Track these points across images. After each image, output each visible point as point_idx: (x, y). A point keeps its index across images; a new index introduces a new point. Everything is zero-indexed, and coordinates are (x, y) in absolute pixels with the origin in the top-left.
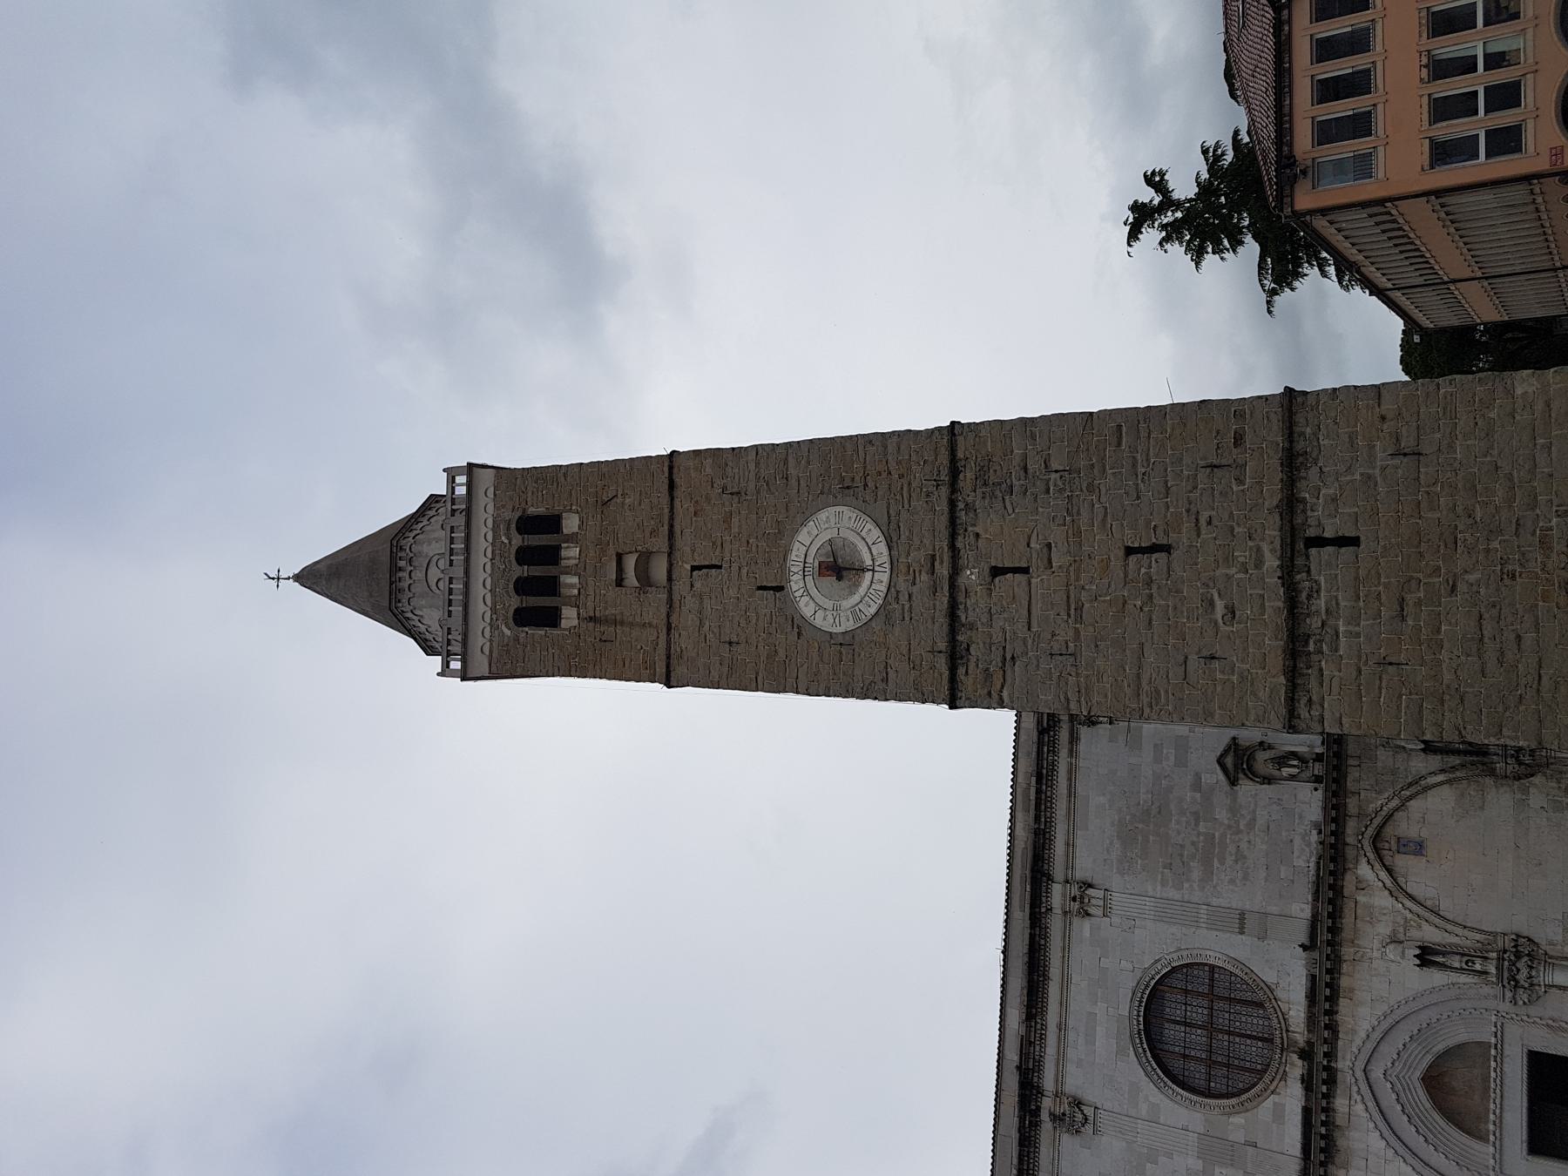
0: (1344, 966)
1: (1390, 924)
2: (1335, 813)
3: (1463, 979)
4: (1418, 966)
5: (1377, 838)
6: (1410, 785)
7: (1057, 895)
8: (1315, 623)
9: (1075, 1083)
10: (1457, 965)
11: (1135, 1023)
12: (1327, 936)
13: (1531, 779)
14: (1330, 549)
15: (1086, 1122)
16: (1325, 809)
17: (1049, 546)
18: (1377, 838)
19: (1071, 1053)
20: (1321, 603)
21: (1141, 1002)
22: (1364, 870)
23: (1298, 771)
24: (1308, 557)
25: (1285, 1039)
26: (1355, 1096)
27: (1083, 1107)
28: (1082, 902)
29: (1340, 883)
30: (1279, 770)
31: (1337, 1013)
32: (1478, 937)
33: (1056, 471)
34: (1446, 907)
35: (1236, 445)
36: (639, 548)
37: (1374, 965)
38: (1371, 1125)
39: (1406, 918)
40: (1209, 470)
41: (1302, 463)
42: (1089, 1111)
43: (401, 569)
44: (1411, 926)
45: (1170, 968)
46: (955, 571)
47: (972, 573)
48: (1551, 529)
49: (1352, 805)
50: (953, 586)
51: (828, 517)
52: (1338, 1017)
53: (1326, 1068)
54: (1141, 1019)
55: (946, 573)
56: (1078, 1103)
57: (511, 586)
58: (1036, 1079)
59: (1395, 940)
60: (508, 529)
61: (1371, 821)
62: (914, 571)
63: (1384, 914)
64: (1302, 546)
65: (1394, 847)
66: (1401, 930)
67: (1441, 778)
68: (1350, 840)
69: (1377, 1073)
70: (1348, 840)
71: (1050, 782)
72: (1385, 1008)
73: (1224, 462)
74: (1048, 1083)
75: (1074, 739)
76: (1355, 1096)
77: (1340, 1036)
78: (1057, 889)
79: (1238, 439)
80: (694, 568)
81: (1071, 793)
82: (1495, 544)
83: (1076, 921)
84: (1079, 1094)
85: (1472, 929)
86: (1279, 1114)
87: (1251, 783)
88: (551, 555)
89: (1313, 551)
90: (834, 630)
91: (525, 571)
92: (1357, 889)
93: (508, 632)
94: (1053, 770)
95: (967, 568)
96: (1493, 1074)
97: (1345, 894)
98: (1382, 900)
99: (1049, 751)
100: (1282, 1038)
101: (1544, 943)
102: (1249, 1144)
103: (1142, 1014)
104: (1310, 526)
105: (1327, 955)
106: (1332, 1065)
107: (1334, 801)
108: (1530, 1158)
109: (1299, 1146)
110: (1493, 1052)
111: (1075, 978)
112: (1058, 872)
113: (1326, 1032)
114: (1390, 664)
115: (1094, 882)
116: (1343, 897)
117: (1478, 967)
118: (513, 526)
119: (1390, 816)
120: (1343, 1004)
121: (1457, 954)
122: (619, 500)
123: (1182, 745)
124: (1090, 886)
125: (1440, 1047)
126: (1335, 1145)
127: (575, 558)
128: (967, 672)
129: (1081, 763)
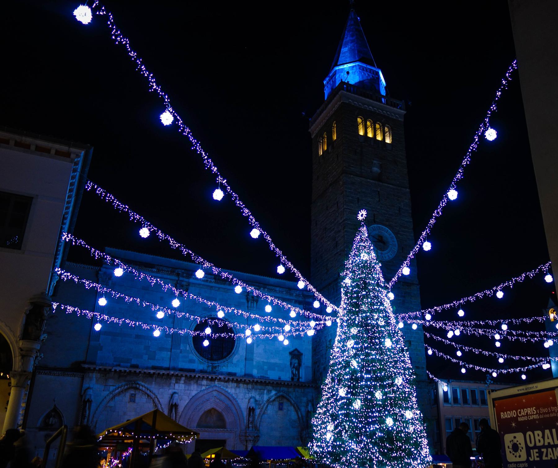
0: (246, 385)
1: (259, 400)
4: (250, 407)
5: (283, 397)
6: (298, 407)
10: (251, 419)
16: (273, 380)
18: (283, 397)
22: (274, 392)
23: (294, 373)
25: (215, 365)
30: (294, 367)
31: (232, 382)
39: (261, 404)
49: (291, 390)
52: (231, 383)
61: (288, 395)
65: (281, 402)
66: (258, 403)
67: (300, 416)
77: (225, 383)
97: (267, 387)
98: (266, 397)
100: (215, 364)
106: (216, 380)
110: (225, 430)
117: (250, 425)
120: (235, 384)
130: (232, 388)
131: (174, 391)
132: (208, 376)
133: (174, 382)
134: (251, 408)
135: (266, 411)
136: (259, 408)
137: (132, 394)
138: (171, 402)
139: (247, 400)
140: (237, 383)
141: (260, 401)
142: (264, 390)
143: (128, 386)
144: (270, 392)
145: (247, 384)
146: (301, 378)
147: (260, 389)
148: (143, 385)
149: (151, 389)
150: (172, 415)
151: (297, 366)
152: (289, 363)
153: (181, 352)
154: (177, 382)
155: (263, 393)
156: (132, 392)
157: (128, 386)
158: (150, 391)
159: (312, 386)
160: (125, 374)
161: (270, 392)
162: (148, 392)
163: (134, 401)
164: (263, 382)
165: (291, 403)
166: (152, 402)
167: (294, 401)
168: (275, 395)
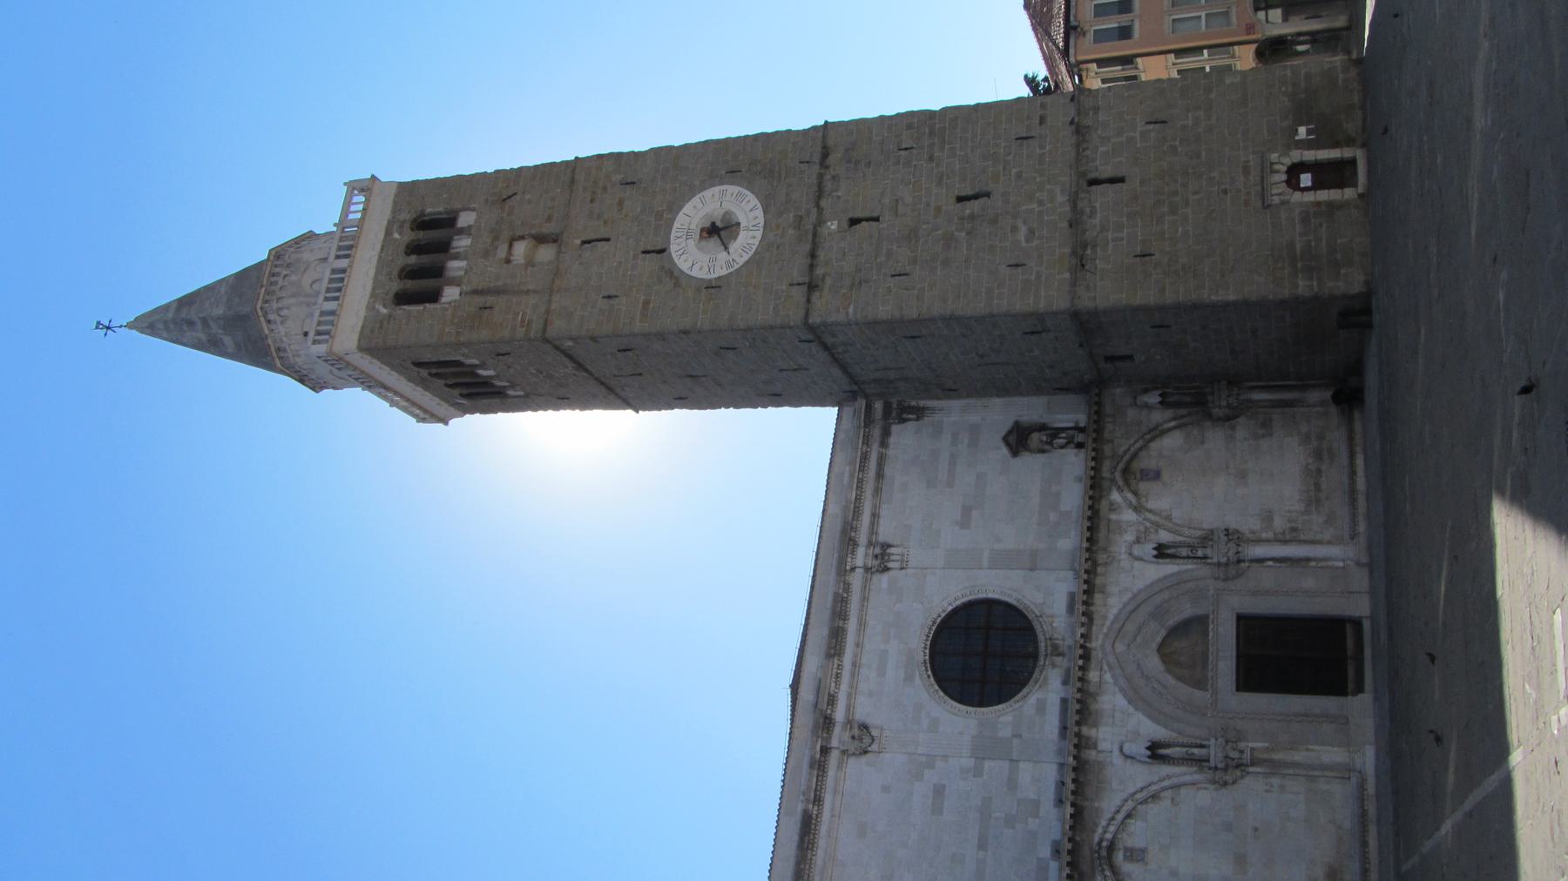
0: (1099, 570)
2: (1097, 459)
3: (1188, 566)
4: (1156, 557)
6: (1150, 431)
7: (861, 557)
8: (1090, 235)
9: (865, 710)
10: (1184, 552)
11: (922, 654)
12: (1085, 545)
13: (1237, 420)
14: (1104, 185)
15: (872, 743)
17: (897, 200)
19: (862, 686)
20: (1097, 221)
21: (928, 636)
22: (1115, 496)
23: (1064, 441)
24: (1089, 192)
26: (1105, 667)
27: (872, 730)
28: (882, 559)
29: (1097, 507)
30: (1050, 443)
31: (1092, 604)
32: (1199, 533)
33: (906, 149)
34: (1176, 514)
35: (1041, 123)
36: (533, 232)
37: (1123, 564)
38: (1117, 689)
39: (1146, 528)
40: (1020, 141)
41: (1086, 132)
42: (875, 733)
43: (273, 275)
44: (1150, 532)
45: (954, 606)
46: (820, 222)
47: (832, 224)
48: (1248, 161)
49: (1107, 449)
50: (815, 235)
51: (713, 195)
53: (1082, 647)
54: (927, 651)
55: (811, 227)
56: (864, 727)
57: (395, 273)
58: (829, 711)
59: (1138, 541)
60: (401, 227)
62: (784, 228)
63: (1130, 526)
64: (1085, 184)
65: (1138, 476)
66: (1143, 536)
67: (1173, 424)
68: (1106, 474)
69: (1120, 647)
70: (1104, 475)
71: (862, 468)
72: (1129, 595)
73: (1030, 135)
74: (839, 715)
75: (886, 433)
76: (1105, 667)
77: (1095, 622)
78: (861, 551)
79: (1042, 120)
80: (584, 242)
81: (880, 475)
82: (1215, 174)
83: (876, 577)
84: (869, 721)
85: (1195, 529)
86: (1041, 708)
87: (1027, 453)
88: (443, 247)
89: (1094, 188)
90: (709, 277)
91: (413, 259)
92: (1110, 509)
93: (384, 311)
94: (865, 458)
95: (830, 221)
96: (1211, 634)
97: (1102, 514)
98: (1129, 516)
99: (863, 443)
101: (1248, 532)
102: (1015, 736)
103: (928, 647)
104: (1091, 172)
105: (1087, 560)
106: (1088, 645)
107: (1094, 445)
108: (1238, 693)
109: (1056, 731)
110: (1211, 617)
111: (871, 622)
112: (862, 538)
113: (1084, 618)
114: (1144, 256)
115: (895, 543)
116: (1099, 517)
117: (1200, 553)
118: (407, 225)
119: (1135, 455)
120: (1098, 597)
121: (1184, 547)
122: (518, 197)
123: (974, 431)
124: (890, 546)
125: (1171, 622)
126: (1088, 708)
127: (467, 246)
128: (821, 296)
129: (890, 452)
130: (1105, 605)
131: (1116, 753)
132: (1077, 668)
133: (1093, 753)
134: (1155, 552)
135: (1164, 514)
136: (1157, 531)
137: (1125, 856)
138: (1143, 759)
139: (1137, 564)
140: (1093, 592)
141: (1138, 531)
142: (1109, 520)
143: (1105, 867)
144: (1115, 506)
145: (1095, 564)
146: (1077, 422)
147: (1109, 531)
148: (1102, 831)
149: (1113, 810)
150: (1177, 756)
151: (1046, 435)
152: (1041, 458)
153: (1019, 736)
154: (1095, 746)
155: (1118, 522)
156: (1119, 857)
157: (1105, 867)
158: (1118, 812)
159: (1098, 395)
160: (1076, 876)
161: (1115, 506)
162: (1120, 817)
163: (1143, 851)
164: (1089, 524)
165: (1140, 449)
166: (1144, 806)
167: (1136, 441)
168: (1122, 491)
